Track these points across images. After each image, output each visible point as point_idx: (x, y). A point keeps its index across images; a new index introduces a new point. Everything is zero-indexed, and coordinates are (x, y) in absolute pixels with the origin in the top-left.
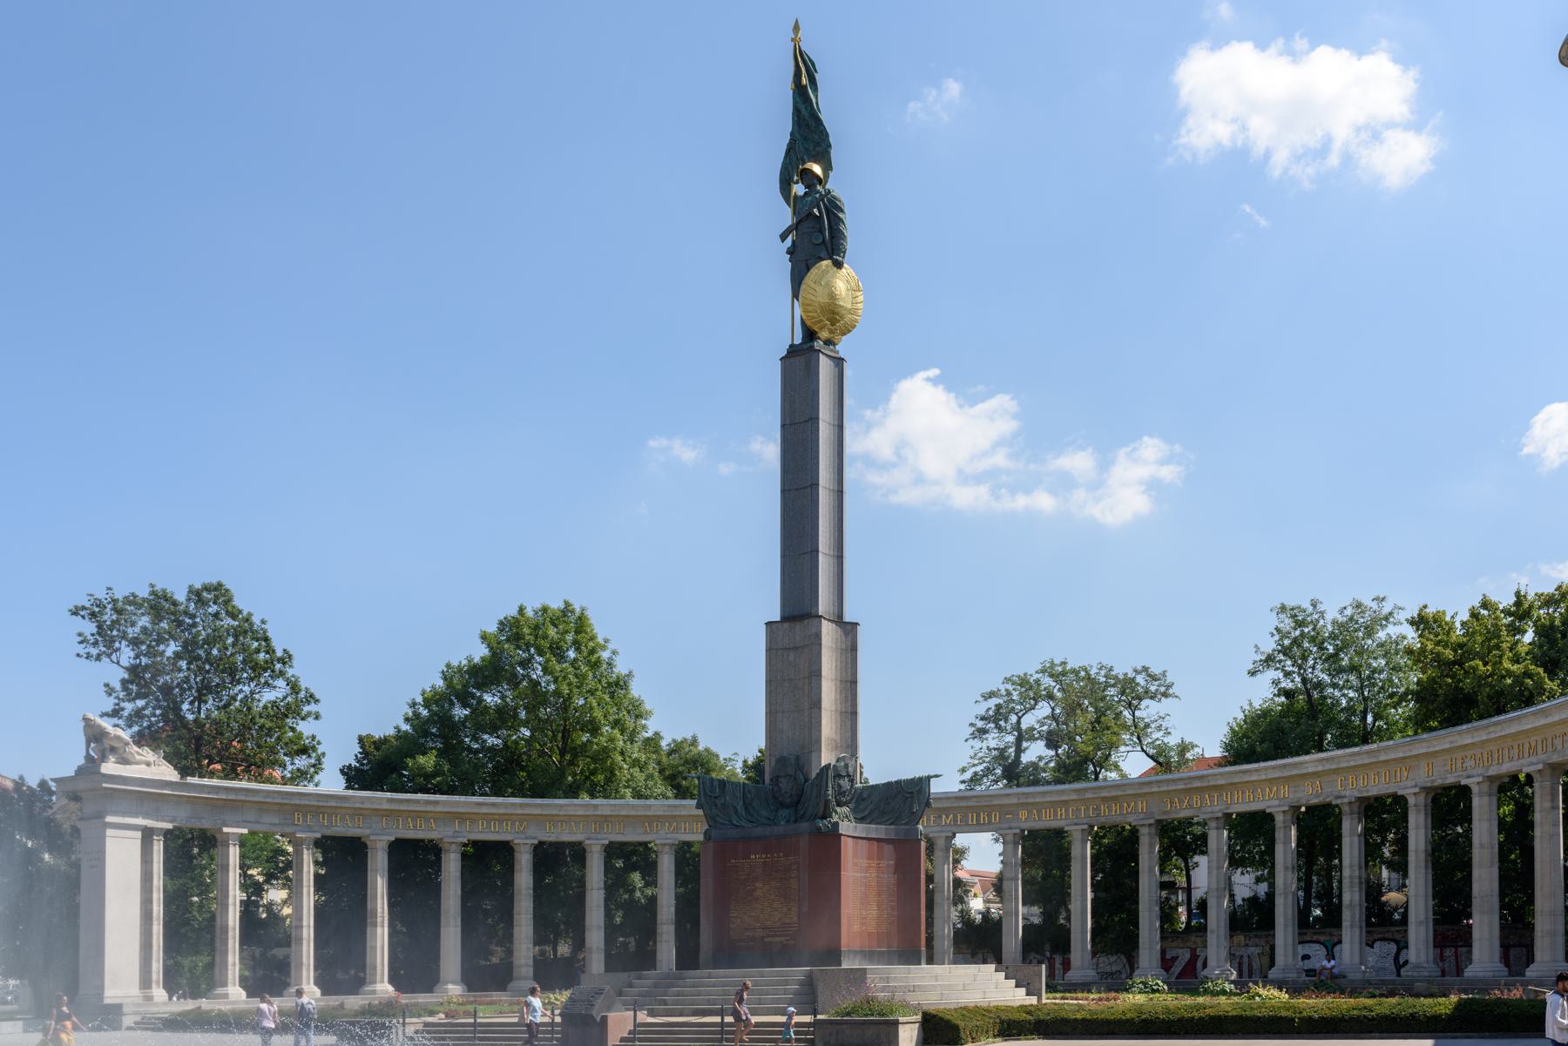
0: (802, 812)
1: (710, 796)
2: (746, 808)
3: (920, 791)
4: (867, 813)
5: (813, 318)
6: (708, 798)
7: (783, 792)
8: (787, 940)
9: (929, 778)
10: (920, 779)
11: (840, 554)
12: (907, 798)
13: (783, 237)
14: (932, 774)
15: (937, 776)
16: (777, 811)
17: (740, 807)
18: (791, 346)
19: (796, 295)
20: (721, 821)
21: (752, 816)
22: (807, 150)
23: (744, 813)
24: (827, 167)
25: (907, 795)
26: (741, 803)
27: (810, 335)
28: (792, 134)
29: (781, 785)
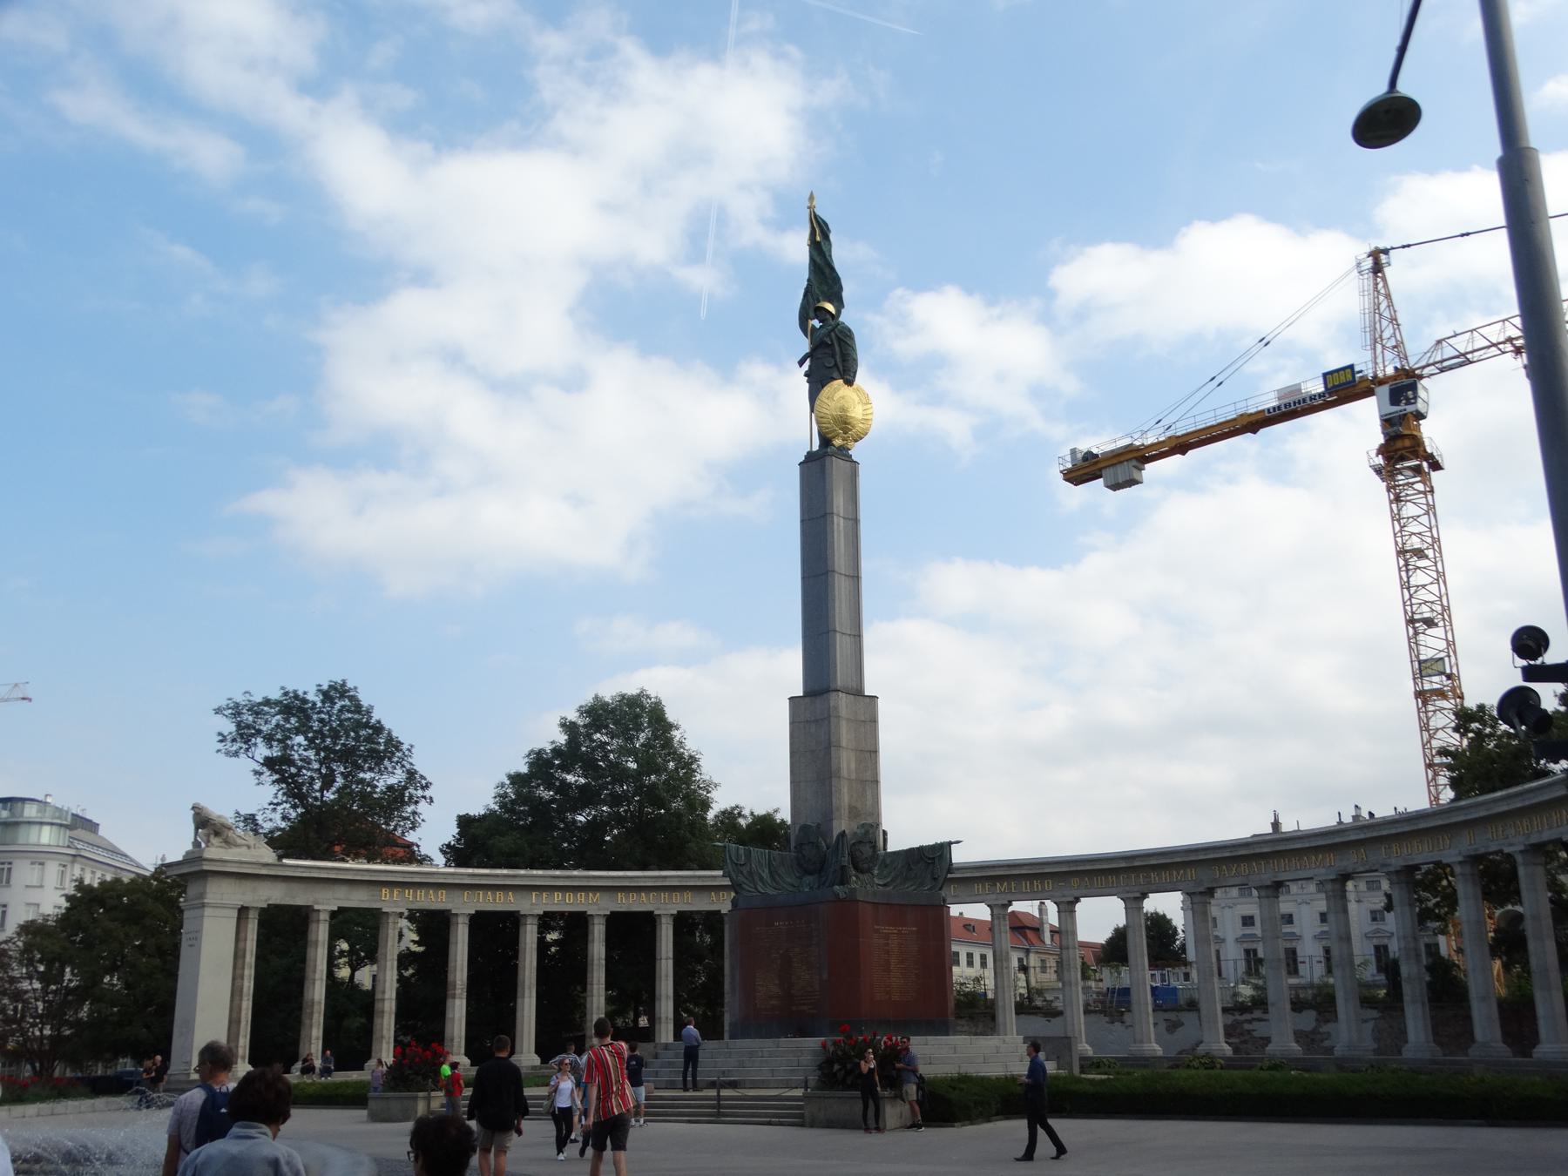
0: (824, 879)
1: (736, 864)
3: (941, 856)
4: (889, 880)
5: (827, 428)
9: (950, 843)
11: (857, 633)
13: (801, 363)
15: (958, 842)
16: (800, 878)
17: (766, 875)
18: (808, 453)
19: (812, 410)
21: (777, 883)
22: (823, 293)
23: (769, 882)
24: (839, 302)
26: (767, 871)
27: (826, 441)
28: (809, 280)
29: (804, 852)
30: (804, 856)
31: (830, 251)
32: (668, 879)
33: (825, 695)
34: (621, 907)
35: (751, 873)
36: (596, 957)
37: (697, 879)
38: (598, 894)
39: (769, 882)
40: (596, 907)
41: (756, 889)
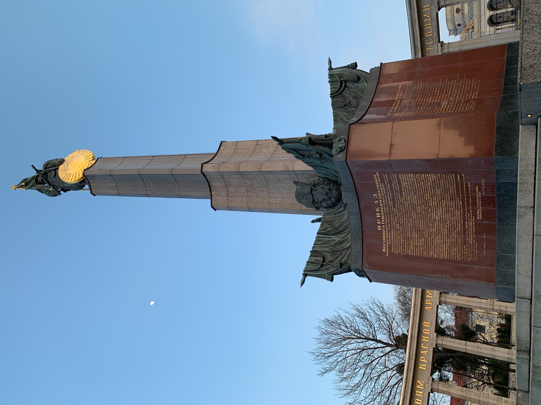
1: (322, 265)
2: (339, 233)
3: (340, 76)
6: (323, 268)
7: (326, 197)
8: (480, 190)
9: (330, 69)
10: (331, 76)
12: (346, 86)
14: (328, 67)
15: (330, 62)
20: (346, 257)
25: (343, 86)
26: (334, 237)
29: (321, 200)
30: (323, 200)
31: (30, 178)
32: (413, 335)
33: (208, 178)
34: (429, 368)
35: (333, 252)
36: (460, 393)
37: (415, 316)
38: (418, 381)
39: (345, 235)
40: (427, 385)
41: (347, 248)
